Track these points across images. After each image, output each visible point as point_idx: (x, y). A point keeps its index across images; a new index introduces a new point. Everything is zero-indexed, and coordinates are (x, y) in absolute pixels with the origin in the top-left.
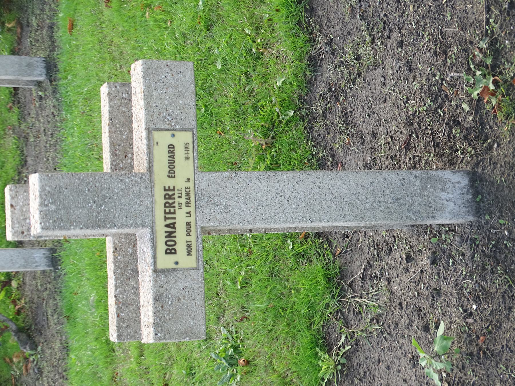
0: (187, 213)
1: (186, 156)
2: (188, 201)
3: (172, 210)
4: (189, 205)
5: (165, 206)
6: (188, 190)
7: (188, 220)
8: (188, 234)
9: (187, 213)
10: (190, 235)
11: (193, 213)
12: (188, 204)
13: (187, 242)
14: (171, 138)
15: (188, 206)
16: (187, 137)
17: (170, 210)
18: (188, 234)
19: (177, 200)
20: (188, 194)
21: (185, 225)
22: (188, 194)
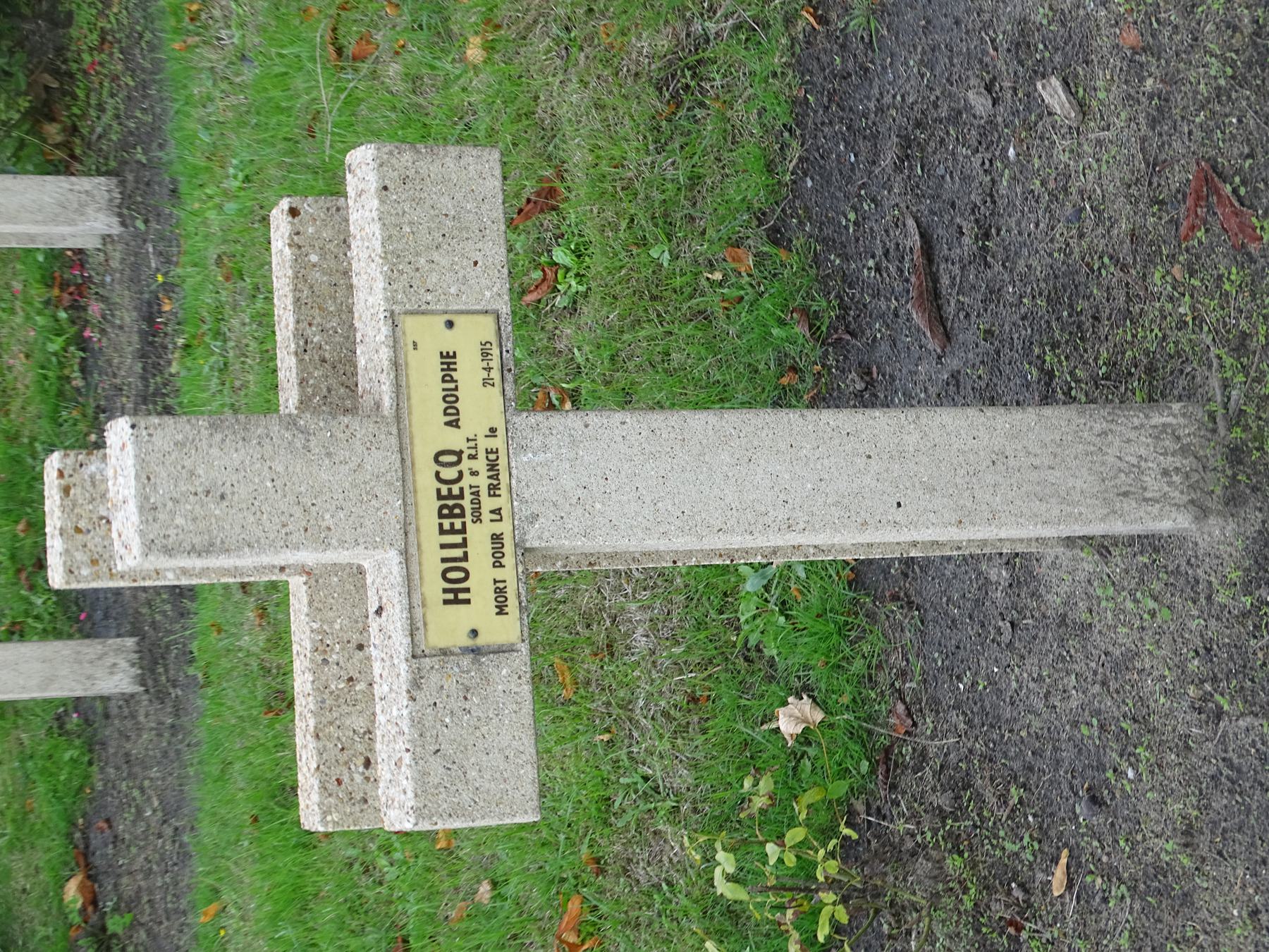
0: (492, 512)
2: (495, 482)
4: (498, 492)
6: (492, 457)
7: (497, 528)
8: (498, 564)
9: (492, 512)
10: (502, 566)
12: (493, 490)
13: (495, 582)
14: (448, 332)
15: (495, 495)
18: (498, 564)
19: (467, 481)
20: (493, 466)
21: (490, 541)
22: (493, 466)
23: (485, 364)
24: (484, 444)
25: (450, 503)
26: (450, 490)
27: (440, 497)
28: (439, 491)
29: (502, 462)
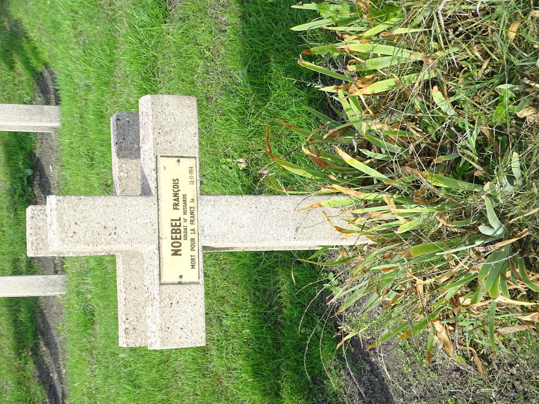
0: (191, 230)
1: (190, 180)
3: (178, 236)
5: (172, 233)
6: (192, 209)
7: (192, 236)
9: (191, 230)
10: (194, 250)
11: (196, 230)
12: (192, 222)
13: (191, 256)
14: (177, 163)
16: (191, 163)
17: (176, 236)
18: (192, 250)
22: (192, 213)
23: (190, 175)
24: (189, 204)
25: (176, 228)
26: (176, 223)
27: (172, 226)
28: (172, 223)
29: (195, 212)
